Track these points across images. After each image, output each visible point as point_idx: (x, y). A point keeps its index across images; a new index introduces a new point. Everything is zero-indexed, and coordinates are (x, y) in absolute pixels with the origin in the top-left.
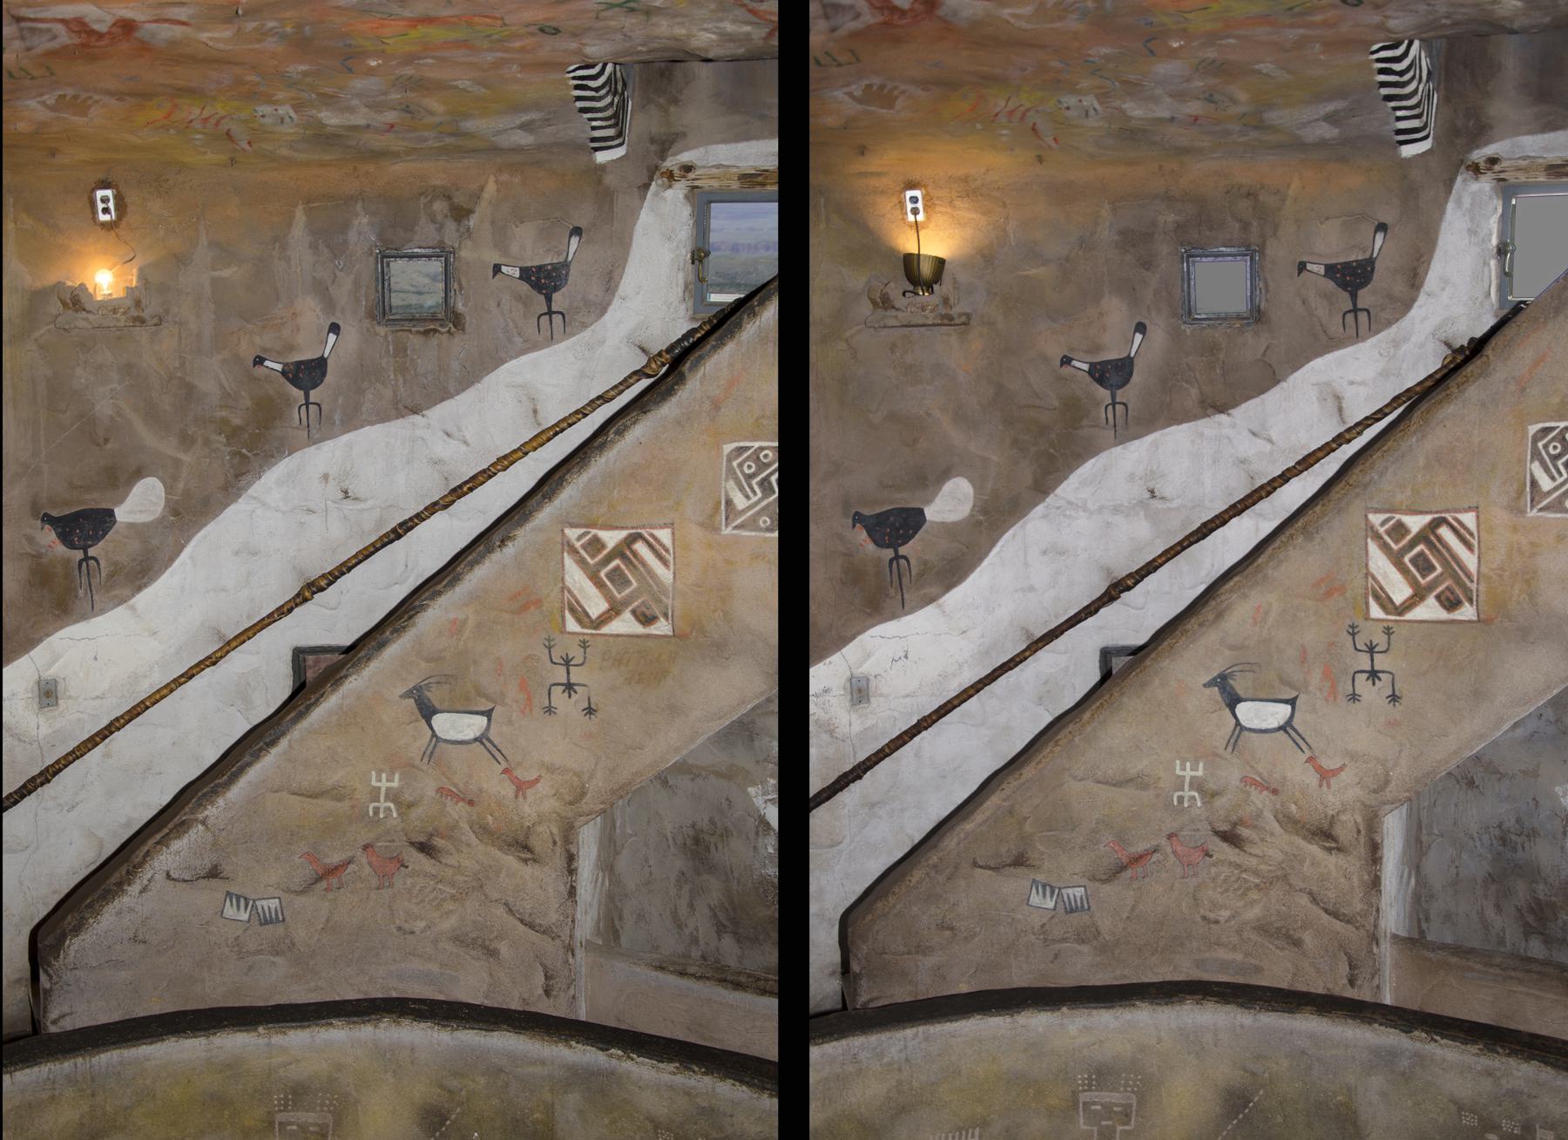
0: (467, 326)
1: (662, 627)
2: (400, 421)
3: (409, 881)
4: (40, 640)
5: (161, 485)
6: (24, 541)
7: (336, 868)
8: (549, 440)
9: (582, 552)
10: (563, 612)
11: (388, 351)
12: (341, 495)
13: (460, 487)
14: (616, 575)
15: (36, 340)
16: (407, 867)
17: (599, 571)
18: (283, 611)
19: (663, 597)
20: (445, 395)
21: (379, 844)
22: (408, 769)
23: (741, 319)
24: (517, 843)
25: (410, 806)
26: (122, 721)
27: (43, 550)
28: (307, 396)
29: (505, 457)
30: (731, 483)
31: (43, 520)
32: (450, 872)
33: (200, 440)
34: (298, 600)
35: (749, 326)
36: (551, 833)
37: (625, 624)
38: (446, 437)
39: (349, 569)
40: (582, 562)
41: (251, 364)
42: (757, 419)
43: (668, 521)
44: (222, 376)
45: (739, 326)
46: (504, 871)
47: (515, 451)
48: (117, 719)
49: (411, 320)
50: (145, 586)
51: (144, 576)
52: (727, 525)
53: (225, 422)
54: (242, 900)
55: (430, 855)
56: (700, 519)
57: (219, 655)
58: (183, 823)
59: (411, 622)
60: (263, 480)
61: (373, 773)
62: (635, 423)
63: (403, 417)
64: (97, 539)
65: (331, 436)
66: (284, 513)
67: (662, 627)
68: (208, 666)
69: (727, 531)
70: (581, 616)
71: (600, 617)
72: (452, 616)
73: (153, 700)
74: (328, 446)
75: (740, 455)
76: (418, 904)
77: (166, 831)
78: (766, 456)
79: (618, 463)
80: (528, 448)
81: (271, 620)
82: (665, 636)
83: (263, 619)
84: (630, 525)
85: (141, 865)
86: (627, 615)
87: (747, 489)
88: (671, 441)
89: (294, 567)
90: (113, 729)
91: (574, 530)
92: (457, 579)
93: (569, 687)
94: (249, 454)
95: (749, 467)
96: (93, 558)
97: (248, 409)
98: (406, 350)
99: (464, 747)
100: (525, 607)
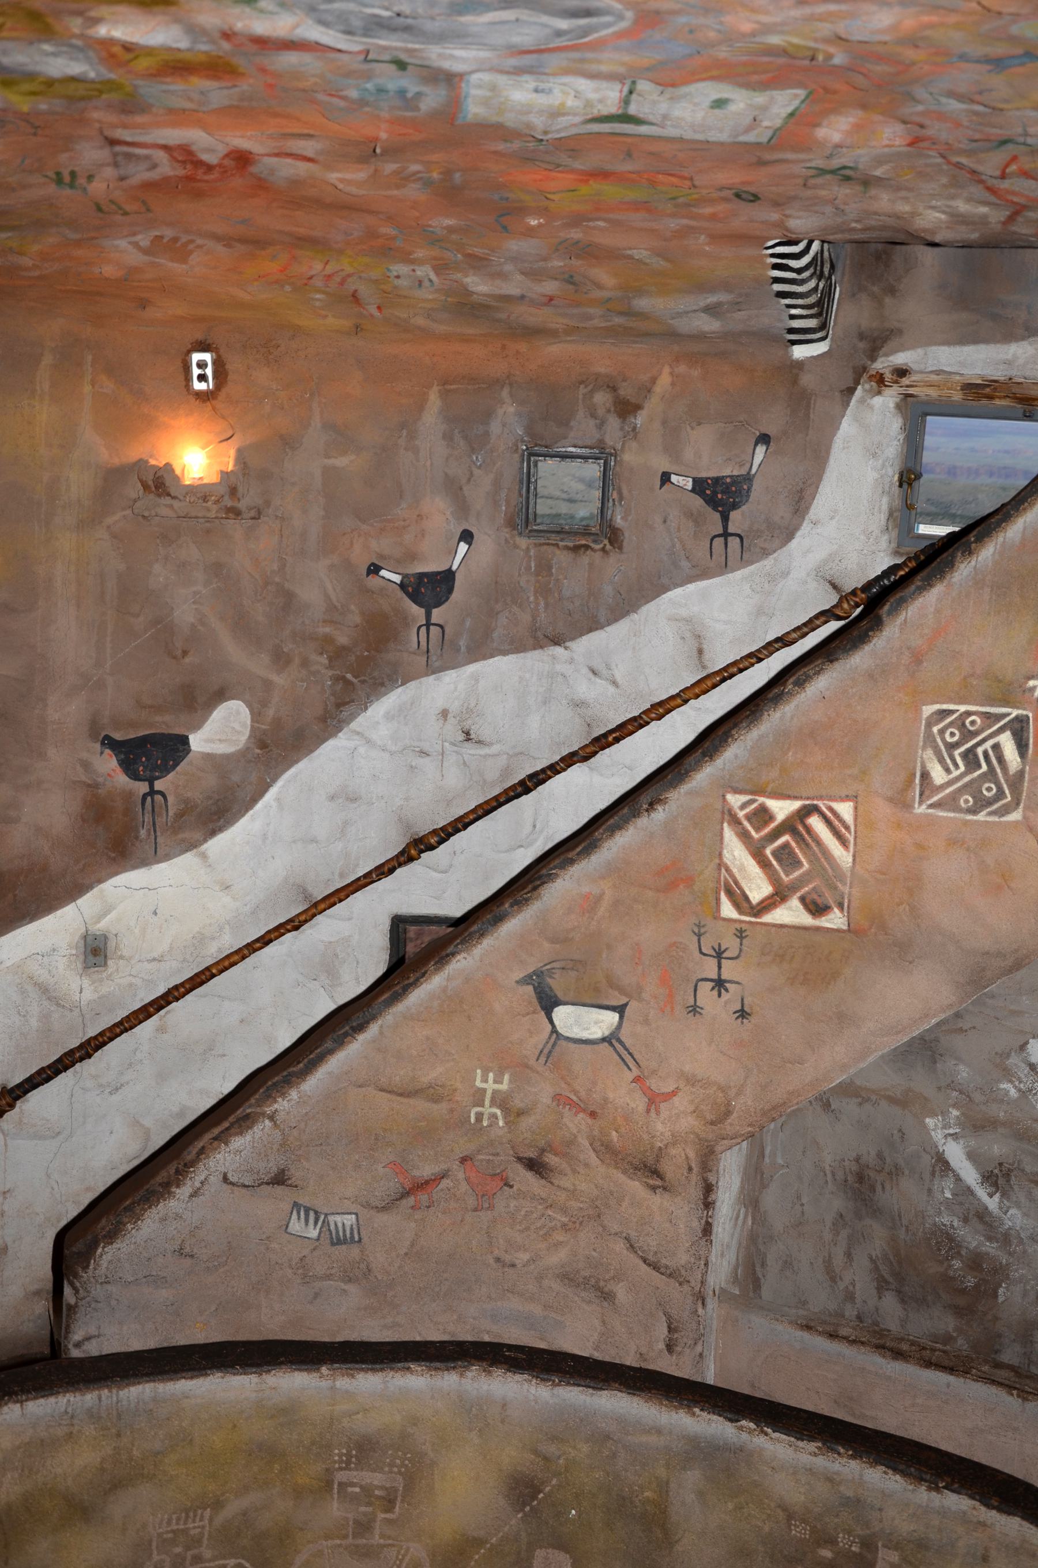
0: (625, 544)
1: (835, 920)
2: (537, 654)
3: (513, 1204)
4: (89, 888)
5: (247, 710)
6: (78, 767)
7: (427, 1182)
8: (715, 686)
9: (746, 824)
10: (718, 893)
11: (528, 568)
12: (461, 737)
13: (605, 735)
14: (785, 855)
16: (511, 1187)
17: (764, 847)
18: (384, 870)
19: (839, 885)
20: (593, 625)
21: (481, 1157)
22: (521, 1069)
23: (954, 557)
24: (645, 1166)
25: (520, 1113)
27: (100, 780)
28: (428, 615)
29: (661, 704)
30: (929, 753)
31: (103, 744)
32: (562, 1196)
34: (402, 859)
35: (962, 566)
36: (687, 1158)
38: (591, 675)
39: (466, 826)
40: (744, 836)
41: (365, 573)
42: (965, 678)
43: (851, 793)
44: (329, 586)
45: (951, 565)
46: (627, 1199)
47: (672, 698)
48: (176, 987)
49: (558, 532)
50: (221, 830)
51: (220, 818)
52: (921, 803)
53: (328, 640)
54: (312, 1215)
55: (540, 1174)
56: (889, 794)
57: (302, 918)
58: (247, 1116)
59: (535, 893)
60: (370, 712)
61: (479, 1071)
62: (818, 673)
63: (542, 647)
64: (166, 770)
66: (392, 753)
67: (835, 920)
68: (289, 931)
69: (920, 809)
70: (740, 900)
71: (762, 902)
72: (586, 889)
73: (220, 967)
74: (450, 677)
75: (941, 720)
76: (521, 1231)
77: (226, 1124)
78: (973, 723)
79: (795, 720)
80: (689, 694)
81: (369, 880)
82: (838, 931)
83: (359, 879)
84: (804, 795)
85: (193, 1163)
86: (795, 902)
87: (948, 761)
88: (860, 698)
89: (400, 819)
90: (171, 999)
91: (737, 796)
92: (593, 847)
93: (720, 984)
94: (355, 680)
95: (952, 734)
97: (357, 626)
98: (550, 568)
99: (589, 1047)
100: (672, 885)
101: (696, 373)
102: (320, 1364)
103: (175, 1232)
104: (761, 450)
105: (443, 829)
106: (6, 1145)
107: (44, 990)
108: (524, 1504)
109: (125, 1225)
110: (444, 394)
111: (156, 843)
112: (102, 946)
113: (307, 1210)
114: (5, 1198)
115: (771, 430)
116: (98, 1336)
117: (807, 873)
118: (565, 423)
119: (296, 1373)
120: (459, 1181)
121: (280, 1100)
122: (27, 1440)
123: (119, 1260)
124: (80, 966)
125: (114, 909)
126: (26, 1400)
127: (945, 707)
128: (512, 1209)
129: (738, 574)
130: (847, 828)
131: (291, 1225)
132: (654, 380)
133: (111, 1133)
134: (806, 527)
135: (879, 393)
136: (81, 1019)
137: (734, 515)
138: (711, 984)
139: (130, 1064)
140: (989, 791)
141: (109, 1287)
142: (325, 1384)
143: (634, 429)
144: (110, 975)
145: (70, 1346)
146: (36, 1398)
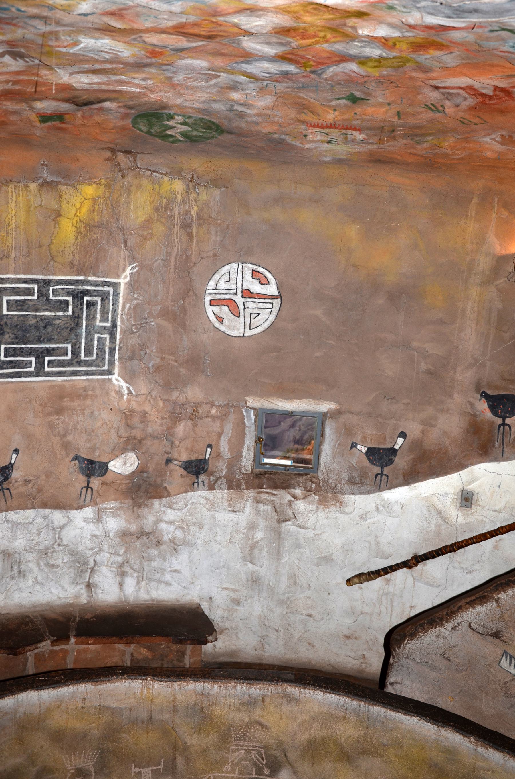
6: (468, 405)
26: (504, 529)
27: (478, 413)
31: (481, 395)
48: (502, 527)
90: (498, 533)
96: (507, 425)
102: (470, 734)
103: (442, 645)
106: (414, 584)
107: (439, 513)
109: (419, 633)
111: (503, 451)
112: (470, 497)
114: (411, 610)
116: (401, 684)
119: (457, 734)
121: (503, 593)
122: (325, 711)
123: (414, 649)
124: (458, 505)
125: (478, 480)
126: (326, 692)
131: (502, 662)
136: (456, 532)
139: (478, 561)
141: (408, 661)
142: (472, 747)
144: (473, 513)
145: (388, 684)
146: (330, 693)
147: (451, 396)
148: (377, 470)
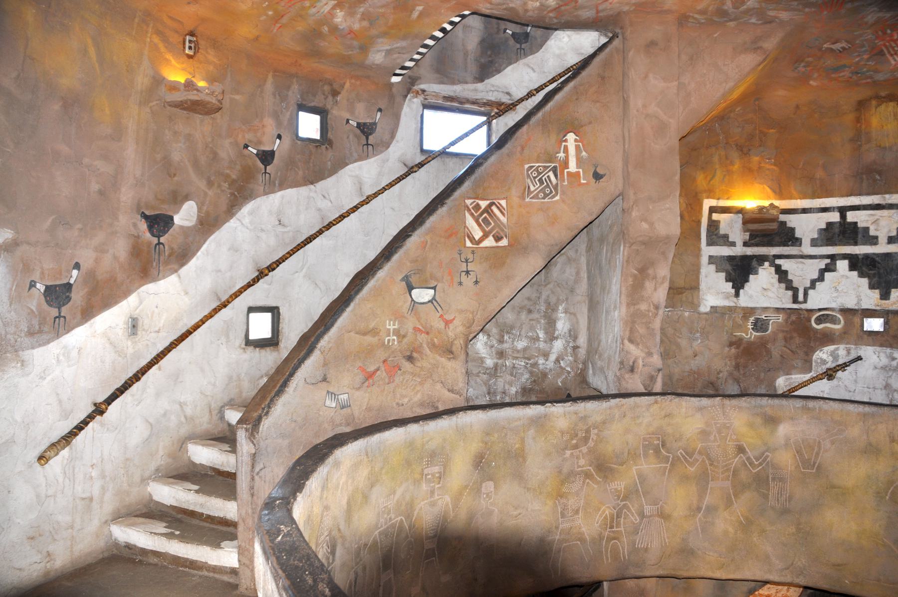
1: (504, 242)
10: (465, 238)
12: (277, 223)
15: (151, 107)
20: (322, 178)
25: (404, 336)
30: (529, 180)
31: (141, 216)
33: (216, 185)
37: (489, 242)
38: (322, 197)
40: (472, 215)
41: (242, 147)
43: (505, 197)
53: (228, 176)
54: (333, 395)
60: (242, 211)
63: (306, 185)
65: (273, 192)
70: (472, 239)
72: (422, 239)
76: (404, 389)
84: (490, 198)
86: (491, 238)
93: (467, 272)
96: (162, 244)
99: (424, 305)
100: (451, 236)
101: (358, 83)
104: (379, 114)
105: (277, 261)
108: (478, 466)
110: (274, 76)
113: (332, 393)
115: (383, 107)
117: (494, 226)
118: (314, 95)
120: (382, 374)
127: (532, 165)
128: (401, 380)
129: (373, 160)
130: (504, 209)
132: (344, 83)
133: (136, 427)
134: (394, 142)
135: (416, 97)
137: (370, 137)
138: (464, 273)
140: (547, 191)
143: (337, 101)
147: (117, 219)
148: (54, 312)
